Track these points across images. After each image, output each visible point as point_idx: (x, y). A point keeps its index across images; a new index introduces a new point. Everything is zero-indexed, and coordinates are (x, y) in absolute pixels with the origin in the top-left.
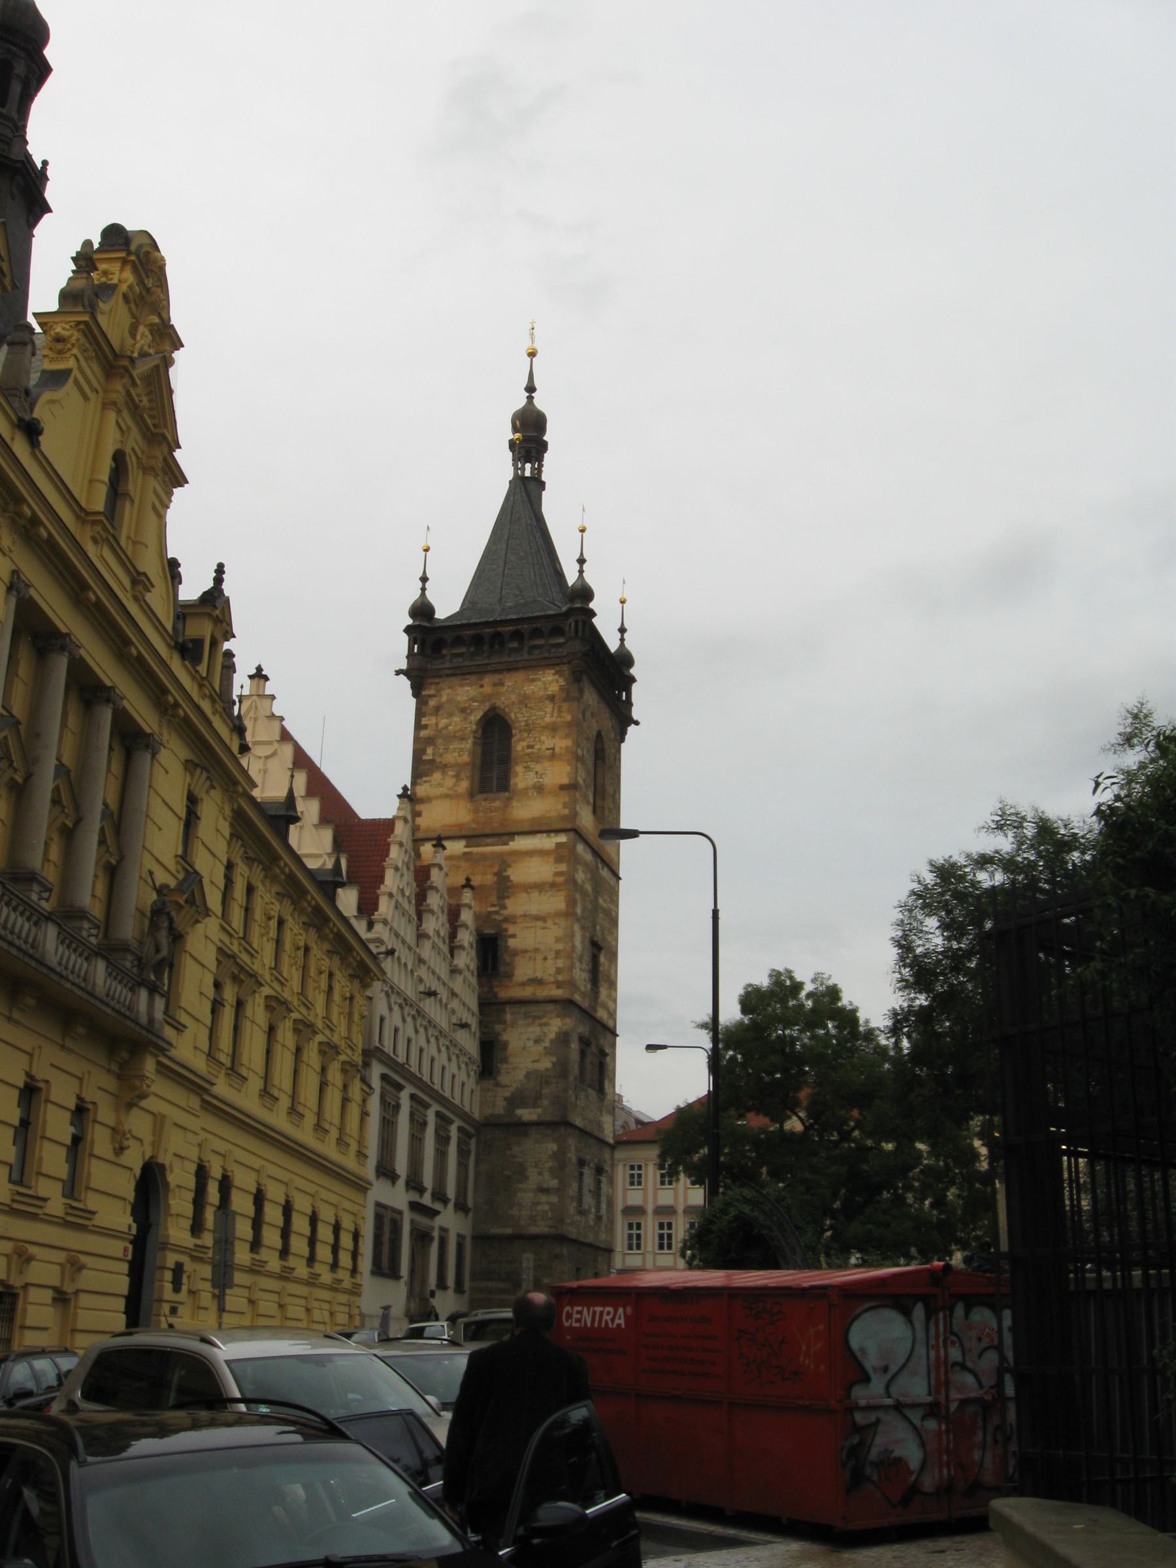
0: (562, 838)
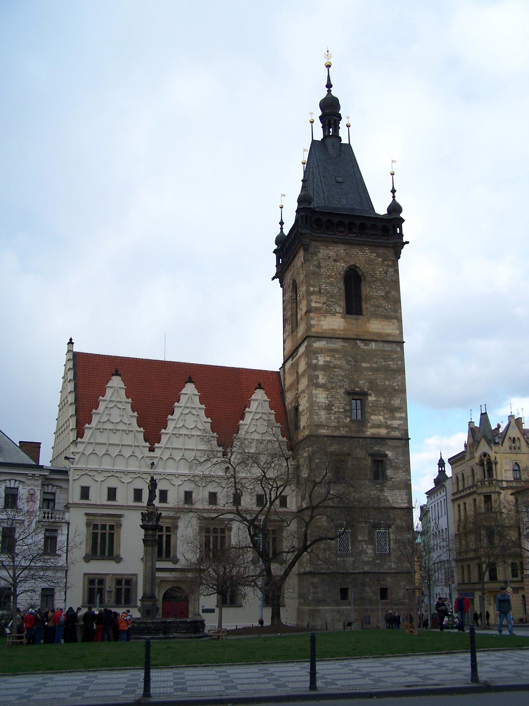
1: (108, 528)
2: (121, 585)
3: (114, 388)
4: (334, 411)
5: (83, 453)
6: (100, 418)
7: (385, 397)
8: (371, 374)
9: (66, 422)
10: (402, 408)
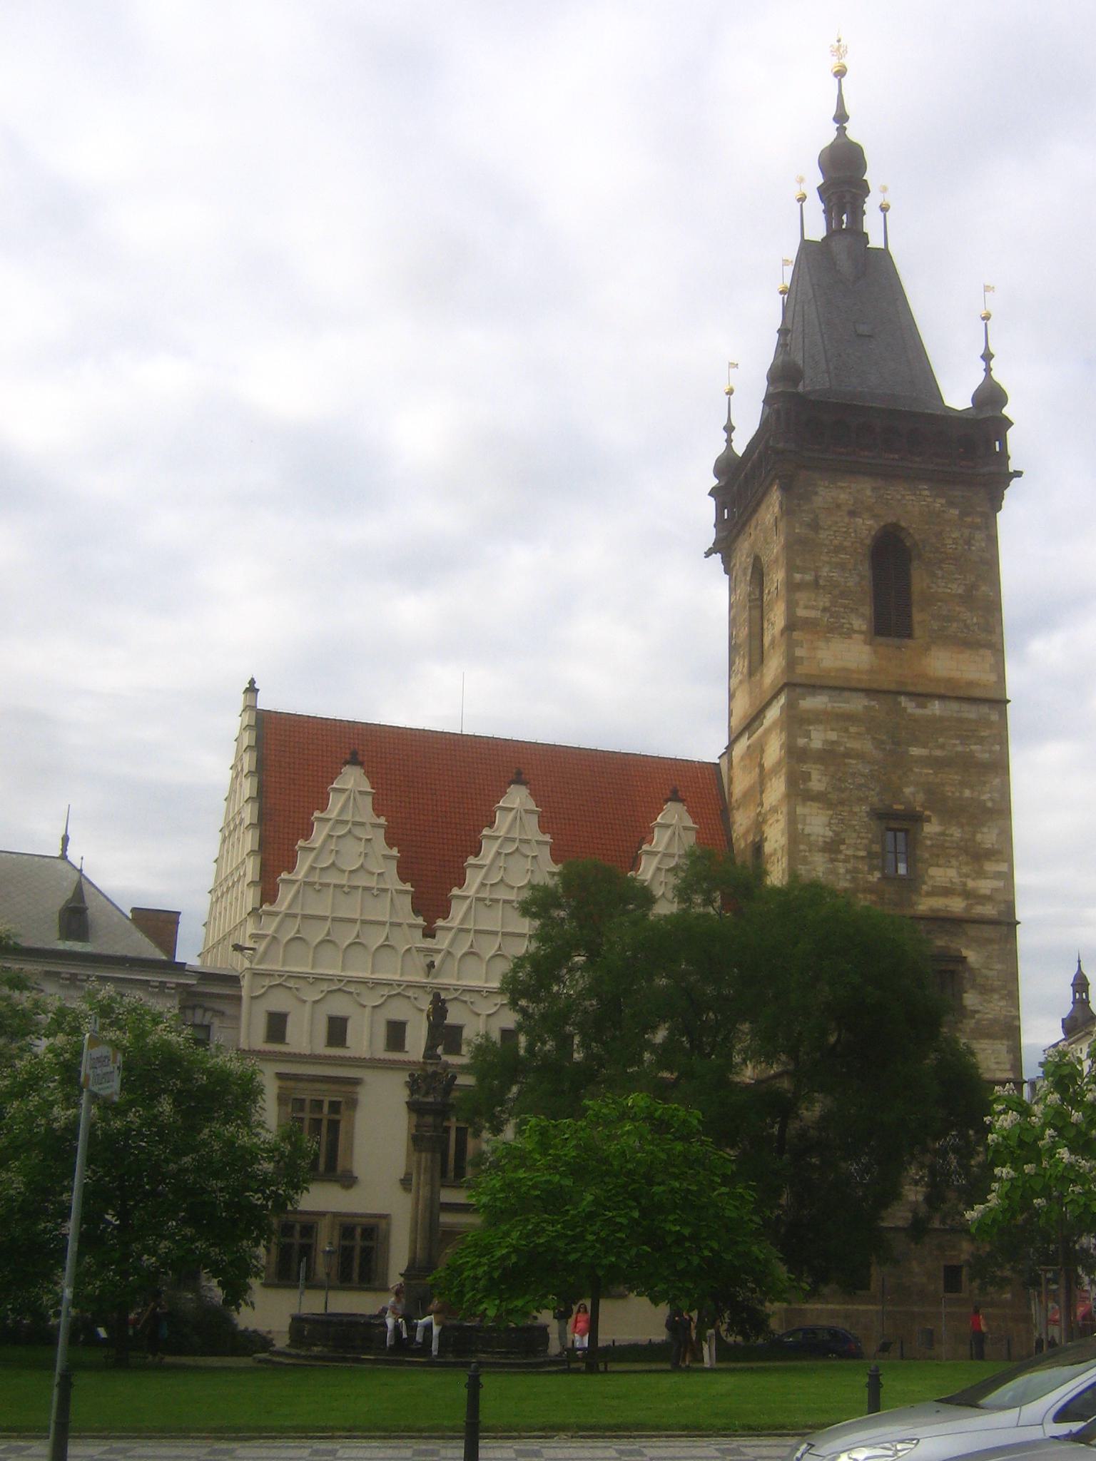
0: (782, 700)
1: (326, 1108)
2: (353, 1238)
3: (347, 793)
4: (846, 855)
5: (274, 938)
6: (316, 859)
7: (961, 826)
8: (931, 771)
9: (237, 868)
10: (999, 852)
